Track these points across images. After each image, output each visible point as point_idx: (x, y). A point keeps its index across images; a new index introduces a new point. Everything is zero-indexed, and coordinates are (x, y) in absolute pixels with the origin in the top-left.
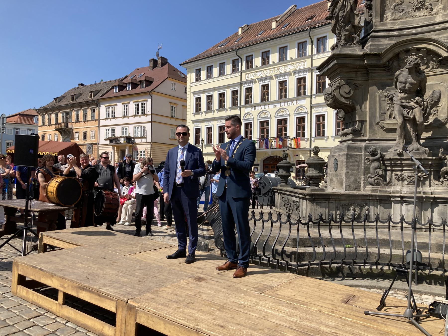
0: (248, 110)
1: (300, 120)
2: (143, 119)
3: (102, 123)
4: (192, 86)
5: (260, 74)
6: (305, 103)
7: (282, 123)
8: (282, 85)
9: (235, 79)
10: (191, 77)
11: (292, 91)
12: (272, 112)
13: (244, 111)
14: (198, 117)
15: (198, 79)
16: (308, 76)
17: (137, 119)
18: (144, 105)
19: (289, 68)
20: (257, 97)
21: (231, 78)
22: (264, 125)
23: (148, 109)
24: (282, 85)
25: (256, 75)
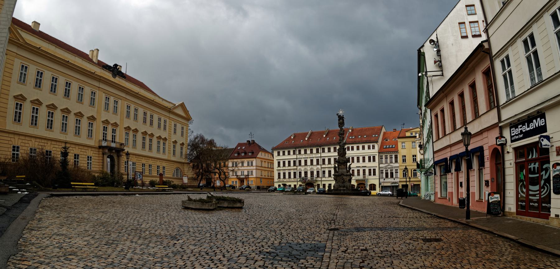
0: (300, 167)
1: (318, 172)
2: (252, 168)
3: (230, 169)
4: (276, 158)
5: (304, 156)
6: (319, 167)
7: (312, 173)
8: (312, 161)
9: (295, 157)
10: (275, 153)
11: (315, 162)
12: (309, 168)
13: (299, 168)
14: (279, 168)
15: (279, 154)
16: (320, 159)
17: (249, 168)
18: (252, 163)
19: (314, 156)
20: (303, 163)
21: (292, 156)
22: (306, 173)
23: (254, 164)
24: (312, 161)
25: (302, 157)
